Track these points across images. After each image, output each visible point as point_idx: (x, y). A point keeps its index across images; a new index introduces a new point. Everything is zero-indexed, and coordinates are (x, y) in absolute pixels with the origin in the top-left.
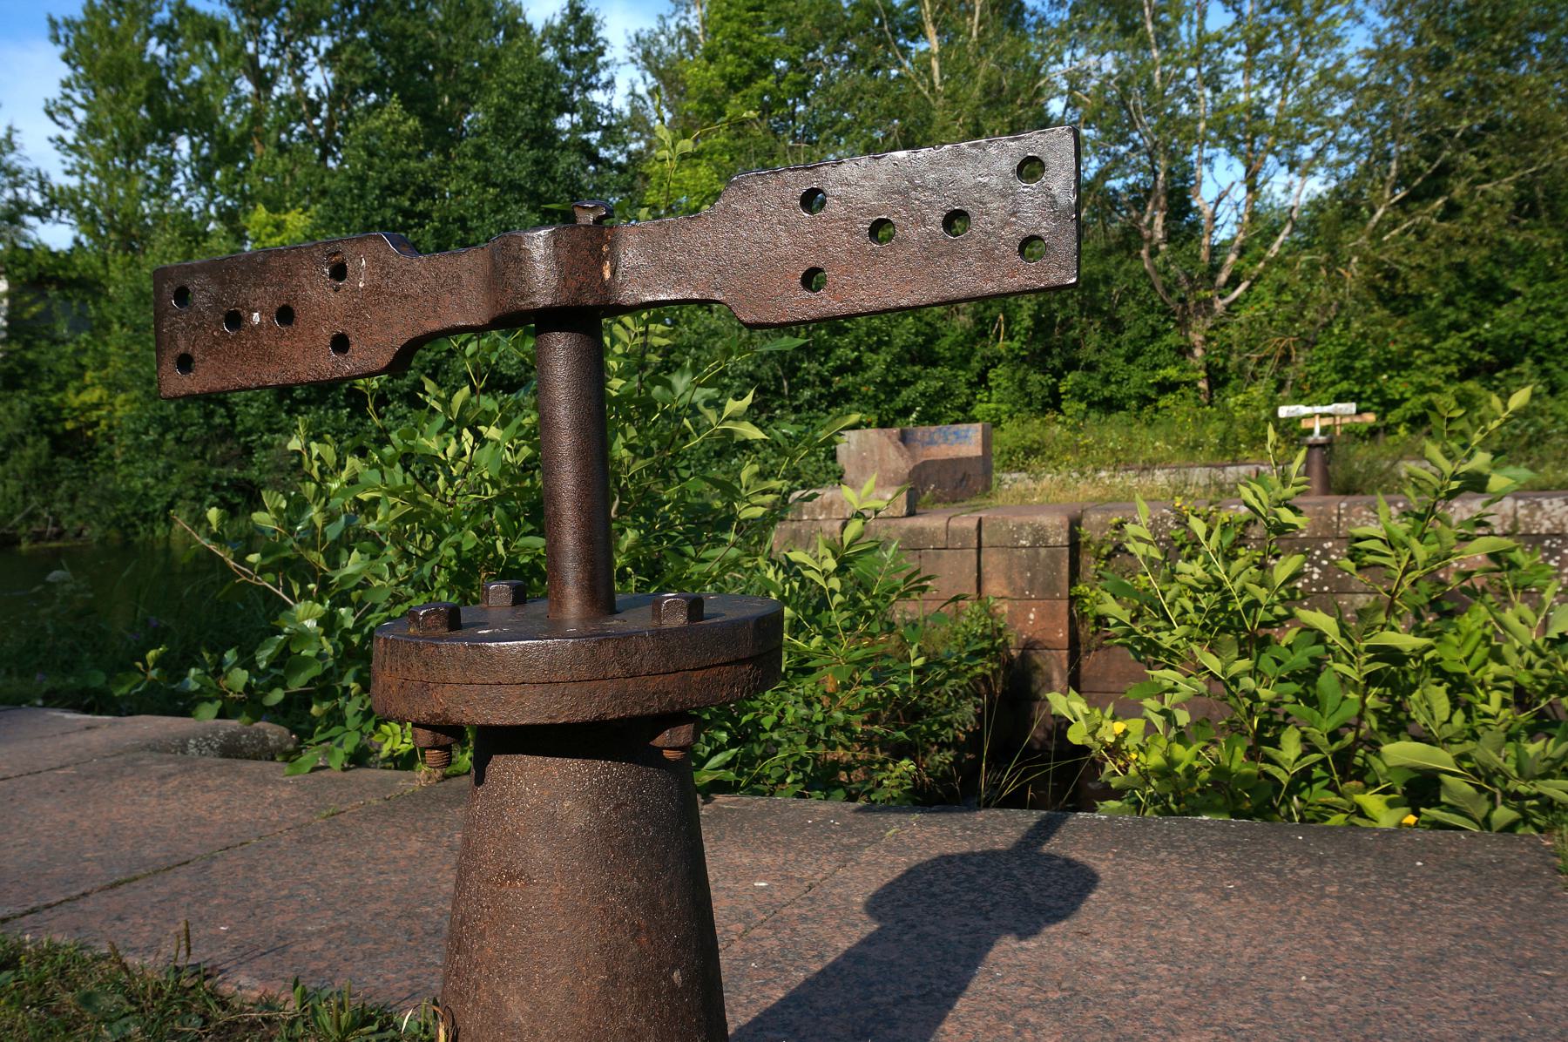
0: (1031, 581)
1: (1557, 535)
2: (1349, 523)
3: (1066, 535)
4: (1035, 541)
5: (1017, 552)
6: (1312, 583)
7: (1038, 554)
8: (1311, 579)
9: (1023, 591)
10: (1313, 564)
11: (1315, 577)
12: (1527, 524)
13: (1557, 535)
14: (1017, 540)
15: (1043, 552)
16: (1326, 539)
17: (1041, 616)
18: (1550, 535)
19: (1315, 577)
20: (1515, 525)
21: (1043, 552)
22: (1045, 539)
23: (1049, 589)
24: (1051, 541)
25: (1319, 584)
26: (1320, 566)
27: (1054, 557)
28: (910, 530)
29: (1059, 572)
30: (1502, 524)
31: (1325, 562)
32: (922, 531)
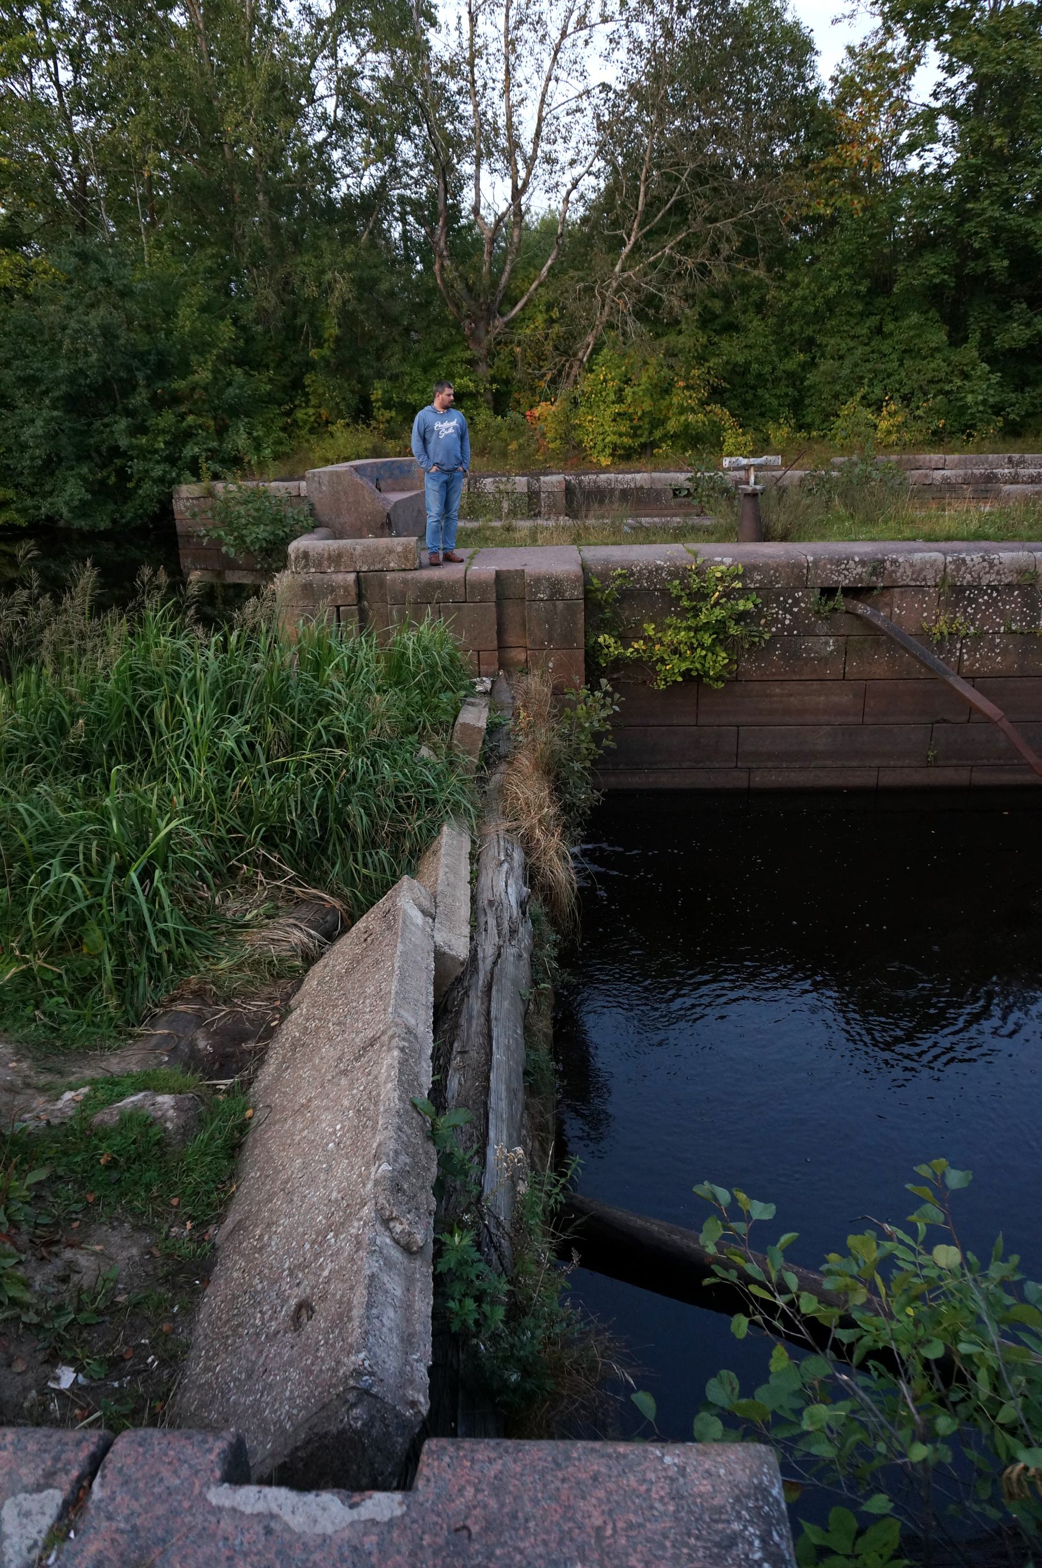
1: (975, 587)
7: (555, 606)
8: (783, 624)
10: (786, 611)
11: (787, 622)
12: (953, 577)
13: (975, 587)
14: (536, 593)
15: (560, 605)
16: (796, 589)
18: (970, 587)
19: (787, 622)
20: (944, 579)
21: (560, 605)
26: (791, 613)
30: (935, 578)
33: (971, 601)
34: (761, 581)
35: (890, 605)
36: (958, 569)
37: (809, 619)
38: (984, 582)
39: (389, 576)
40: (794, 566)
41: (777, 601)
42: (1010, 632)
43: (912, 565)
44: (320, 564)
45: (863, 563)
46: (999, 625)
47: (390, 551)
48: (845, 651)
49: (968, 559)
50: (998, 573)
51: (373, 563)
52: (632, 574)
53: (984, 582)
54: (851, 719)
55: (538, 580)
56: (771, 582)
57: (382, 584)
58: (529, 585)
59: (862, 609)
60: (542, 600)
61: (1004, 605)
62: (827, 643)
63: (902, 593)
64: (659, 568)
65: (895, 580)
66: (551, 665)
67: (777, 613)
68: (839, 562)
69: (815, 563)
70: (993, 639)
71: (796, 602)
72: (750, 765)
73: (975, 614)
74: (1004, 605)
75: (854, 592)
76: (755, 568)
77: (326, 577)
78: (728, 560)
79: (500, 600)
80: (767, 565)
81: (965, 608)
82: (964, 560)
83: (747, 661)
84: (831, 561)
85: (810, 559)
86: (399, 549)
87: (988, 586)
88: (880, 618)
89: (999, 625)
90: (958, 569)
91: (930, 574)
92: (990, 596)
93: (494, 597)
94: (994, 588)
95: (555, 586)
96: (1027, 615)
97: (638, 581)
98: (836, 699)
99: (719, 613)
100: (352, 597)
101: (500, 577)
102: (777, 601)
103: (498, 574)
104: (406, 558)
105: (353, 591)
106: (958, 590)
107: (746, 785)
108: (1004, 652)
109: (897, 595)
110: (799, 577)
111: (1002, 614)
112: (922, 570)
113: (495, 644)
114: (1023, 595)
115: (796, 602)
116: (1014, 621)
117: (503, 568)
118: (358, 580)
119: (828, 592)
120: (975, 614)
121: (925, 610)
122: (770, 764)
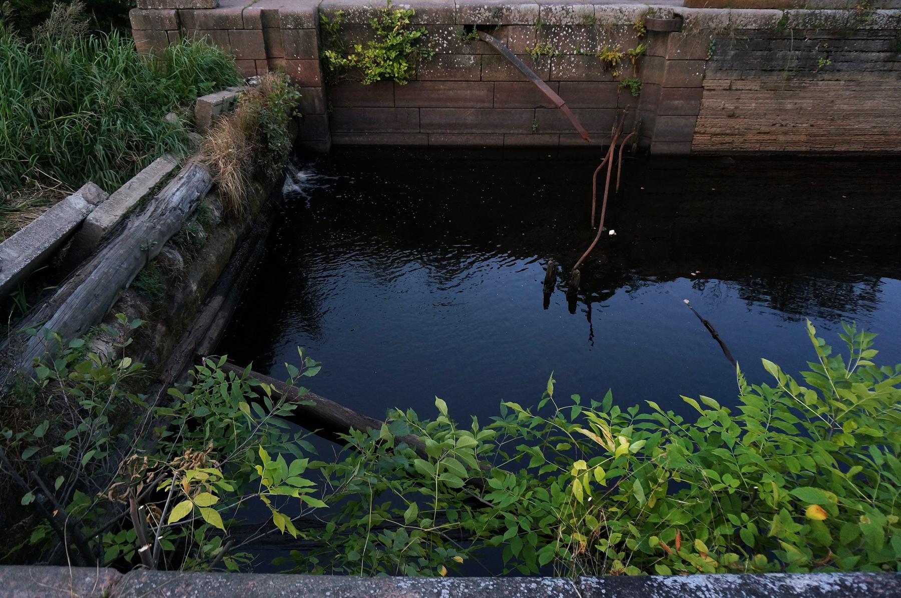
0: (297, 49)
1: (558, 26)
5: (286, 32)
10: (444, 39)
12: (544, 19)
13: (558, 26)
14: (286, 25)
16: (449, 25)
18: (555, 26)
20: (539, 20)
22: (301, 24)
23: (307, 54)
24: (305, 25)
25: (447, 50)
27: (308, 36)
29: (312, 44)
33: (556, 35)
34: (427, 20)
35: (507, 36)
36: (547, 15)
38: (564, 23)
40: (447, 10)
41: (438, 32)
42: (579, 54)
43: (519, 12)
45: (489, 10)
46: (573, 50)
48: (480, 63)
49: (553, 8)
50: (571, 17)
52: (349, 14)
53: (564, 23)
54: (486, 105)
55: (286, 16)
57: (193, 17)
59: (489, 38)
60: (290, 29)
61: (576, 36)
62: (470, 59)
64: (365, 11)
65: (509, 21)
68: (475, 9)
69: (460, 9)
70: (570, 58)
71: (450, 33)
72: (428, 131)
73: (558, 43)
74: (576, 36)
75: (482, 28)
76: (424, 11)
77: (157, 11)
79: (265, 28)
80: (431, 9)
81: (552, 39)
82: (551, 9)
83: (422, 68)
84: (470, 8)
85: (458, 6)
87: (566, 25)
88: (499, 44)
89: (573, 50)
90: (547, 15)
91: (530, 18)
92: (567, 31)
93: (260, 26)
94: (570, 27)
95: (298, 20)
96: (589, 44)
97: (353, 18)
98: (477, 93)
99: (400, 39)
101: (263, 12)
102: (438, 32)
103: (262, 11)
105: (174, 21)
106: (549, 27)
107: (426, 143)
108: (577, 66)
110: (451, 18)
111: (574, 43)
112: (525, 15)
113: (264, 56)
114: (587, 32)
115: (450, 33)
116: (583, 47)
117: (267, 8)
118: (178, 15)
119: (469, 28)
120: (558, 43)
121: (528, 39)
122: (440, 131)
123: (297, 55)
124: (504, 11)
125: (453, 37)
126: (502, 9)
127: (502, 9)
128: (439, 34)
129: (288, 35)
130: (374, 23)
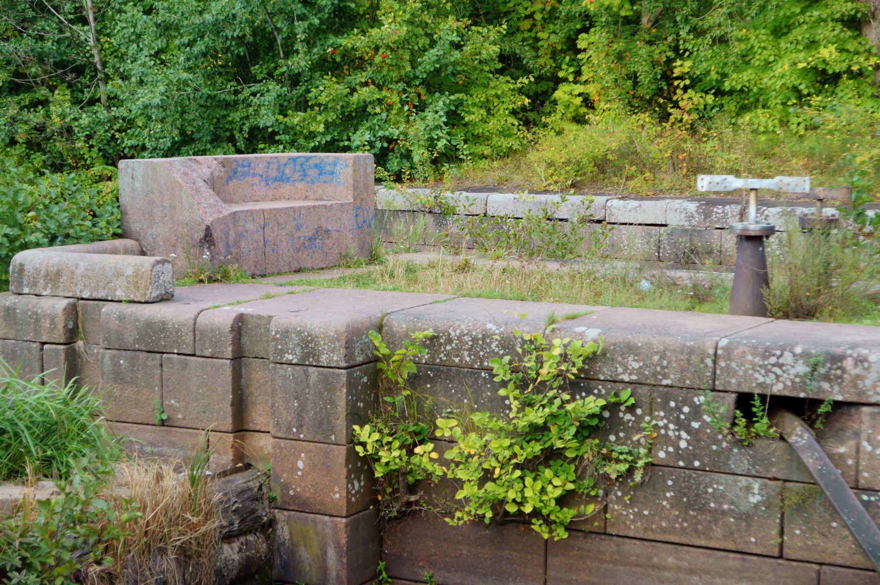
0: (300, 413)
2: (728, 370)
3: (343, 351)
4: (305, 356)
5: (282, 370)
6: (678, 454)
8: (678, 448)
9: (290, 428)
10: (682, 425)
14: (282, 352)
17: (312, 466)
25: (689, 456)
27: (327, 383)
28: (149, 324)
29: (333, 403)
31: (695, 425)
32: (162, 327)
34: (639, 371)
35: (857, 434)
37: (718, 443)
39: (107, 308)
40: (691, 351)
41: (665, 406)
44: (34, 284)
47: (119, 274)
51: (96, 288)
55: (285, 334)
56: (655, 375)
58: (275, 339)
63: (873, 416)
65: (862, 393)
66: (300, 464)
67: (666, 427)
68: (766, 353)
69: (728, 349)
71: (696, 413)
76: (630, 349)
78: (592, 333)
79: (238, 357)
80: (649, 345)
84: (754, 350)
86: (129, 271)
93: (229, 351)
95: (309, 347)
97: (457, 352)
100: (59, 335)
103: (241, 319)
104: (136, 286)
109: (866, 419)
115: (696, 413)
117: (247, 310)
119: (744, 401)
123: (300, 427)
124: (848, 364)
125: (705, 425)
126: (842, 358)
127: (842, 358)
128: (669, 411)
129: (285, 378)
130: (500, 369)
